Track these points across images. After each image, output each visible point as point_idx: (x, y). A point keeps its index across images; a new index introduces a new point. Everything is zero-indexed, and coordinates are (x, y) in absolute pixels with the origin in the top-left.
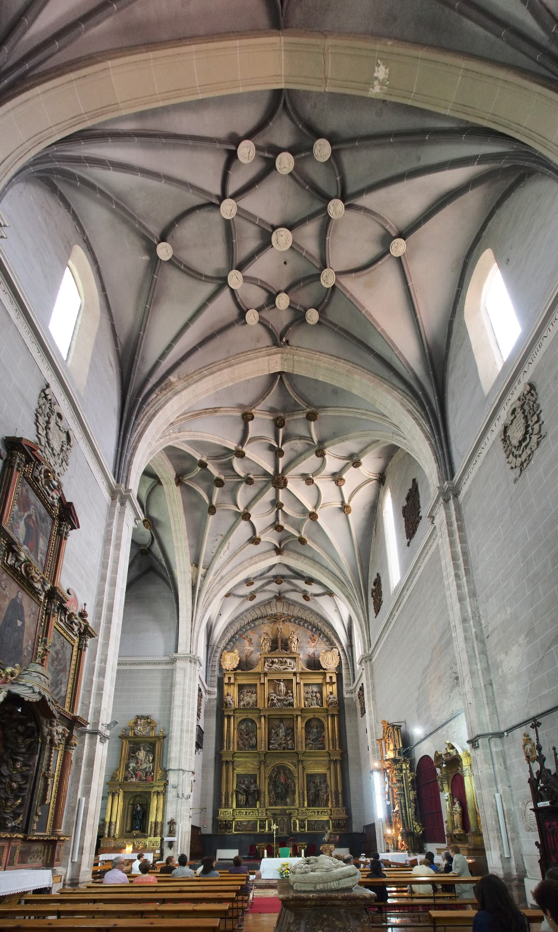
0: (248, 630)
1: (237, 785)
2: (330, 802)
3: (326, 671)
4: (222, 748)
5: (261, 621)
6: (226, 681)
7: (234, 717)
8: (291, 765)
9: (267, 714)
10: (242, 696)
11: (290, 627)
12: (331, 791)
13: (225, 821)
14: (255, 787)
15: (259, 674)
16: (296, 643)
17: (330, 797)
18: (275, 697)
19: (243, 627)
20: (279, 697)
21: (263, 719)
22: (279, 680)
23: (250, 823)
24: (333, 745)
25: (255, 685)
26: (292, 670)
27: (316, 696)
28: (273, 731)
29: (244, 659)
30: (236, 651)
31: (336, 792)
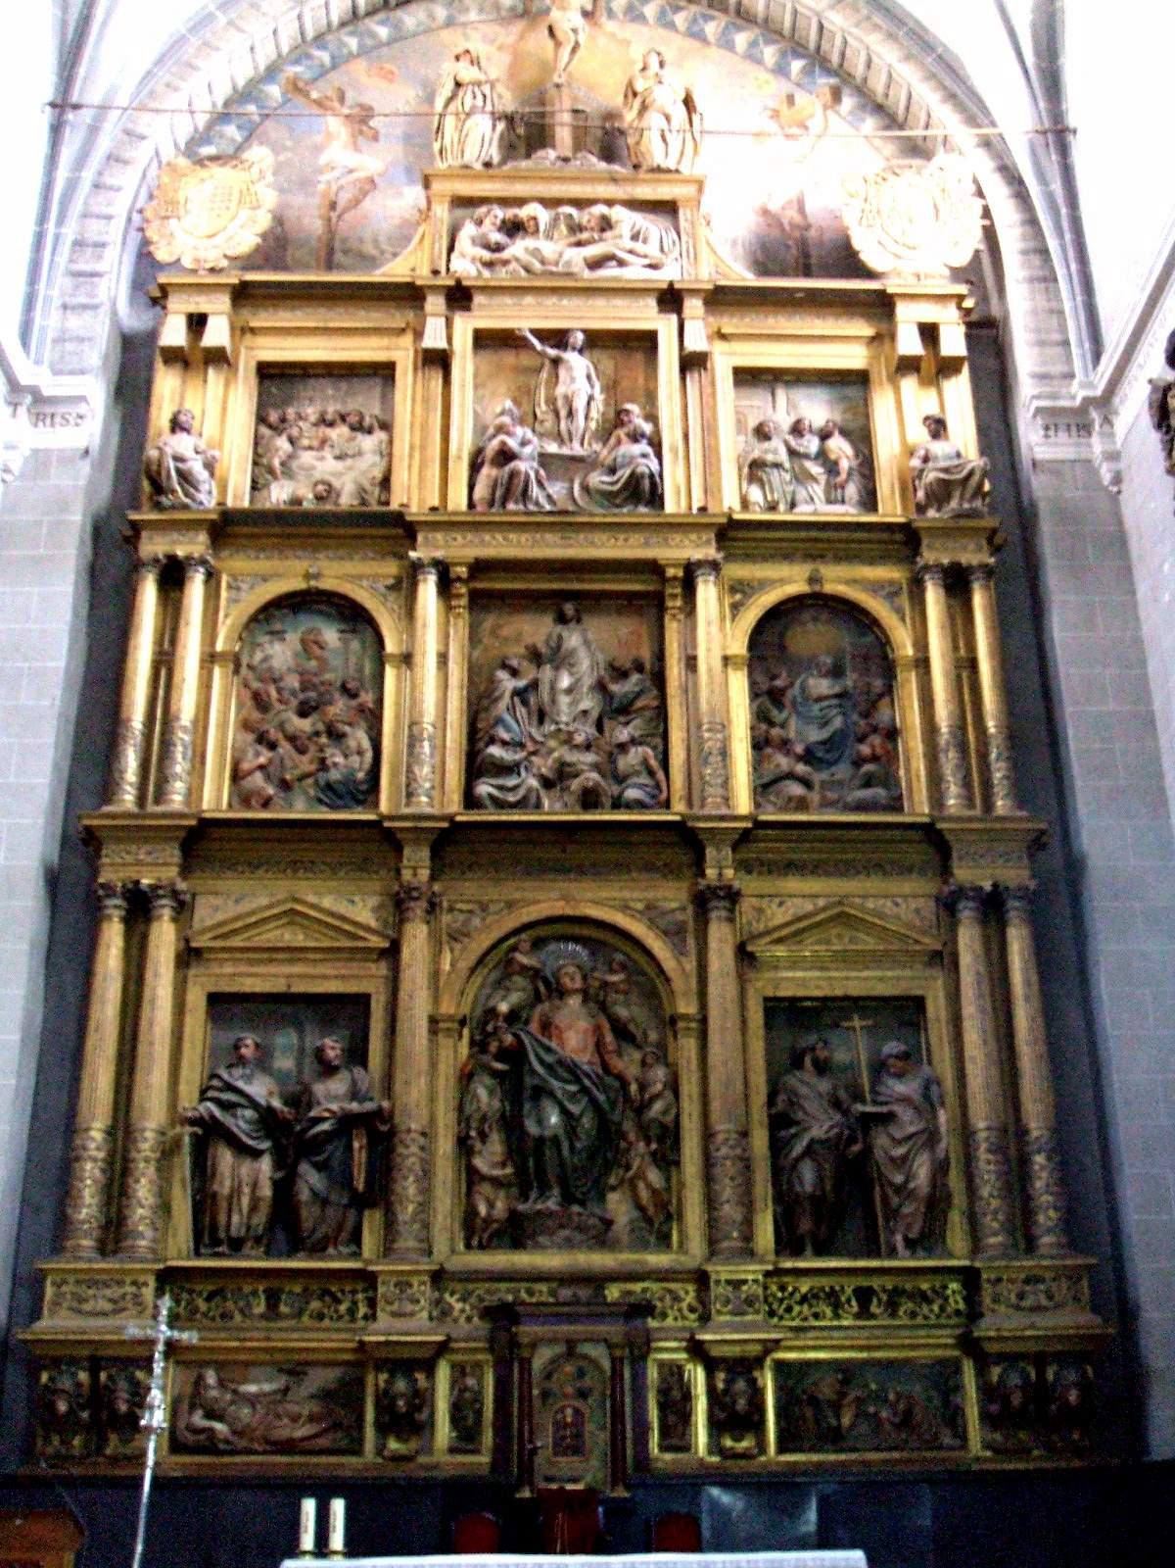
0: (351, 56)
2: (956, 1219)
4: (107, 788)
7: (211, 576)
9: (463, 550)
10: (282, 444)
12: (966, 1133)
14: (354, 1095)
15: (410, 295)
16: (679, 113)
17: (955, 1181)
19: (320, 39)
20: (552, 448)
21: (428, 590)
22: (558, 338)
25: (384, 372)
27: (822, 456)
29: (314, 225)
31: (1012, 1133)
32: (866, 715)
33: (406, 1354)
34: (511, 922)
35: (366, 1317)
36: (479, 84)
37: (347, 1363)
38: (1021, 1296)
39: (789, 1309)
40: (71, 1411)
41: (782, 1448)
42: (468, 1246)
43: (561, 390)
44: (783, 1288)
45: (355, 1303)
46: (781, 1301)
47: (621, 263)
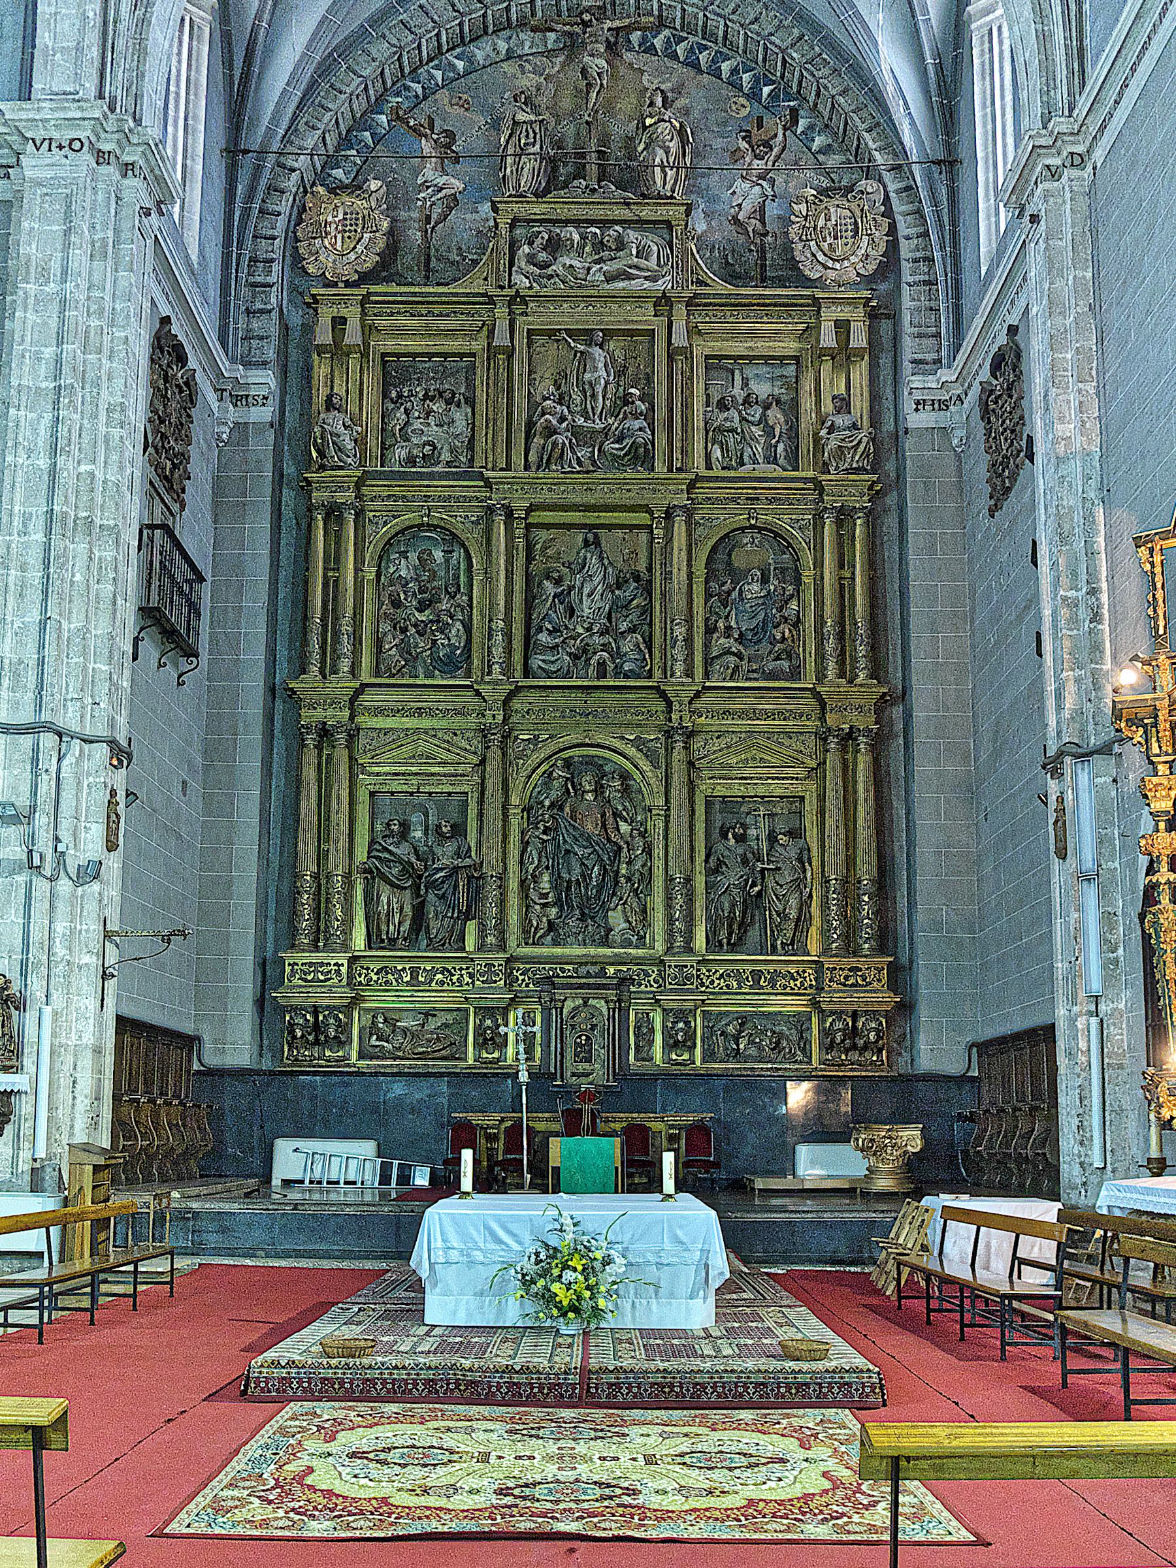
1: (372, 842)
3: (819, 294)
5: (503, 46)
6: (324, 336)
8: (632, 751)
10: (400, 414)
11: (645, 77)
13: (316, 1011)
16: (674, 145)
17: (815, 909)
18: (562, 419)
20: (581, 421)
22: (587, 336)
23: (433, 1024)
24: (841, 662)
26: (647, 284)
27: (763, 419)
28: (549, 587)
30: (374, 185)
31: (848, 884)
32: (780, 609)
33: (490, 1004)
34: (551, 747)
35: (467, 984)
36: (531, 123)
37: (458, 1009)
38: (846, 978)
39: (712, 982)
40: (303, 1036)
41: (704, 1061)
42: (526, 944)
43: (587, 376)
44: (709, 971)
45: (462, 976)
46: (708, 977)
47: (630, 277)
